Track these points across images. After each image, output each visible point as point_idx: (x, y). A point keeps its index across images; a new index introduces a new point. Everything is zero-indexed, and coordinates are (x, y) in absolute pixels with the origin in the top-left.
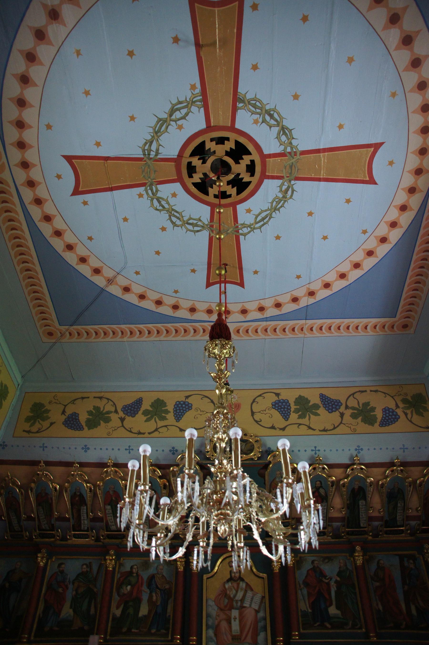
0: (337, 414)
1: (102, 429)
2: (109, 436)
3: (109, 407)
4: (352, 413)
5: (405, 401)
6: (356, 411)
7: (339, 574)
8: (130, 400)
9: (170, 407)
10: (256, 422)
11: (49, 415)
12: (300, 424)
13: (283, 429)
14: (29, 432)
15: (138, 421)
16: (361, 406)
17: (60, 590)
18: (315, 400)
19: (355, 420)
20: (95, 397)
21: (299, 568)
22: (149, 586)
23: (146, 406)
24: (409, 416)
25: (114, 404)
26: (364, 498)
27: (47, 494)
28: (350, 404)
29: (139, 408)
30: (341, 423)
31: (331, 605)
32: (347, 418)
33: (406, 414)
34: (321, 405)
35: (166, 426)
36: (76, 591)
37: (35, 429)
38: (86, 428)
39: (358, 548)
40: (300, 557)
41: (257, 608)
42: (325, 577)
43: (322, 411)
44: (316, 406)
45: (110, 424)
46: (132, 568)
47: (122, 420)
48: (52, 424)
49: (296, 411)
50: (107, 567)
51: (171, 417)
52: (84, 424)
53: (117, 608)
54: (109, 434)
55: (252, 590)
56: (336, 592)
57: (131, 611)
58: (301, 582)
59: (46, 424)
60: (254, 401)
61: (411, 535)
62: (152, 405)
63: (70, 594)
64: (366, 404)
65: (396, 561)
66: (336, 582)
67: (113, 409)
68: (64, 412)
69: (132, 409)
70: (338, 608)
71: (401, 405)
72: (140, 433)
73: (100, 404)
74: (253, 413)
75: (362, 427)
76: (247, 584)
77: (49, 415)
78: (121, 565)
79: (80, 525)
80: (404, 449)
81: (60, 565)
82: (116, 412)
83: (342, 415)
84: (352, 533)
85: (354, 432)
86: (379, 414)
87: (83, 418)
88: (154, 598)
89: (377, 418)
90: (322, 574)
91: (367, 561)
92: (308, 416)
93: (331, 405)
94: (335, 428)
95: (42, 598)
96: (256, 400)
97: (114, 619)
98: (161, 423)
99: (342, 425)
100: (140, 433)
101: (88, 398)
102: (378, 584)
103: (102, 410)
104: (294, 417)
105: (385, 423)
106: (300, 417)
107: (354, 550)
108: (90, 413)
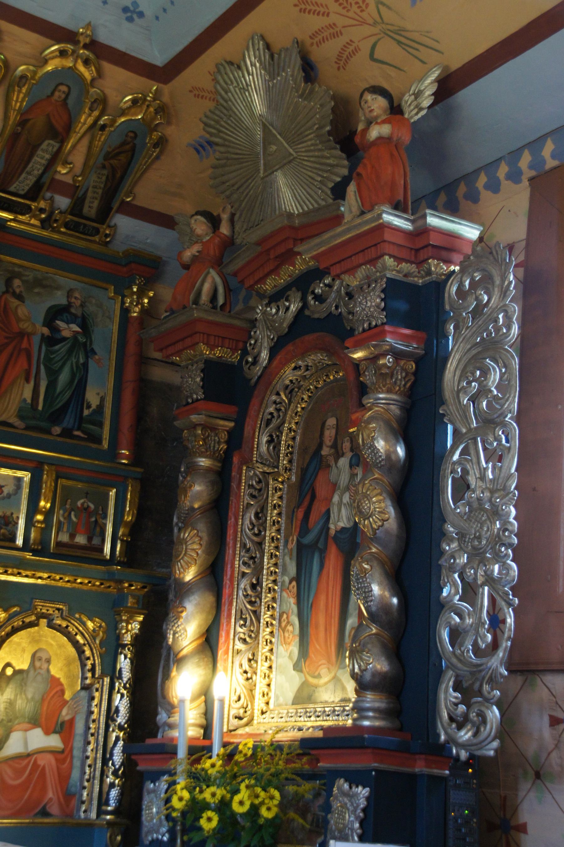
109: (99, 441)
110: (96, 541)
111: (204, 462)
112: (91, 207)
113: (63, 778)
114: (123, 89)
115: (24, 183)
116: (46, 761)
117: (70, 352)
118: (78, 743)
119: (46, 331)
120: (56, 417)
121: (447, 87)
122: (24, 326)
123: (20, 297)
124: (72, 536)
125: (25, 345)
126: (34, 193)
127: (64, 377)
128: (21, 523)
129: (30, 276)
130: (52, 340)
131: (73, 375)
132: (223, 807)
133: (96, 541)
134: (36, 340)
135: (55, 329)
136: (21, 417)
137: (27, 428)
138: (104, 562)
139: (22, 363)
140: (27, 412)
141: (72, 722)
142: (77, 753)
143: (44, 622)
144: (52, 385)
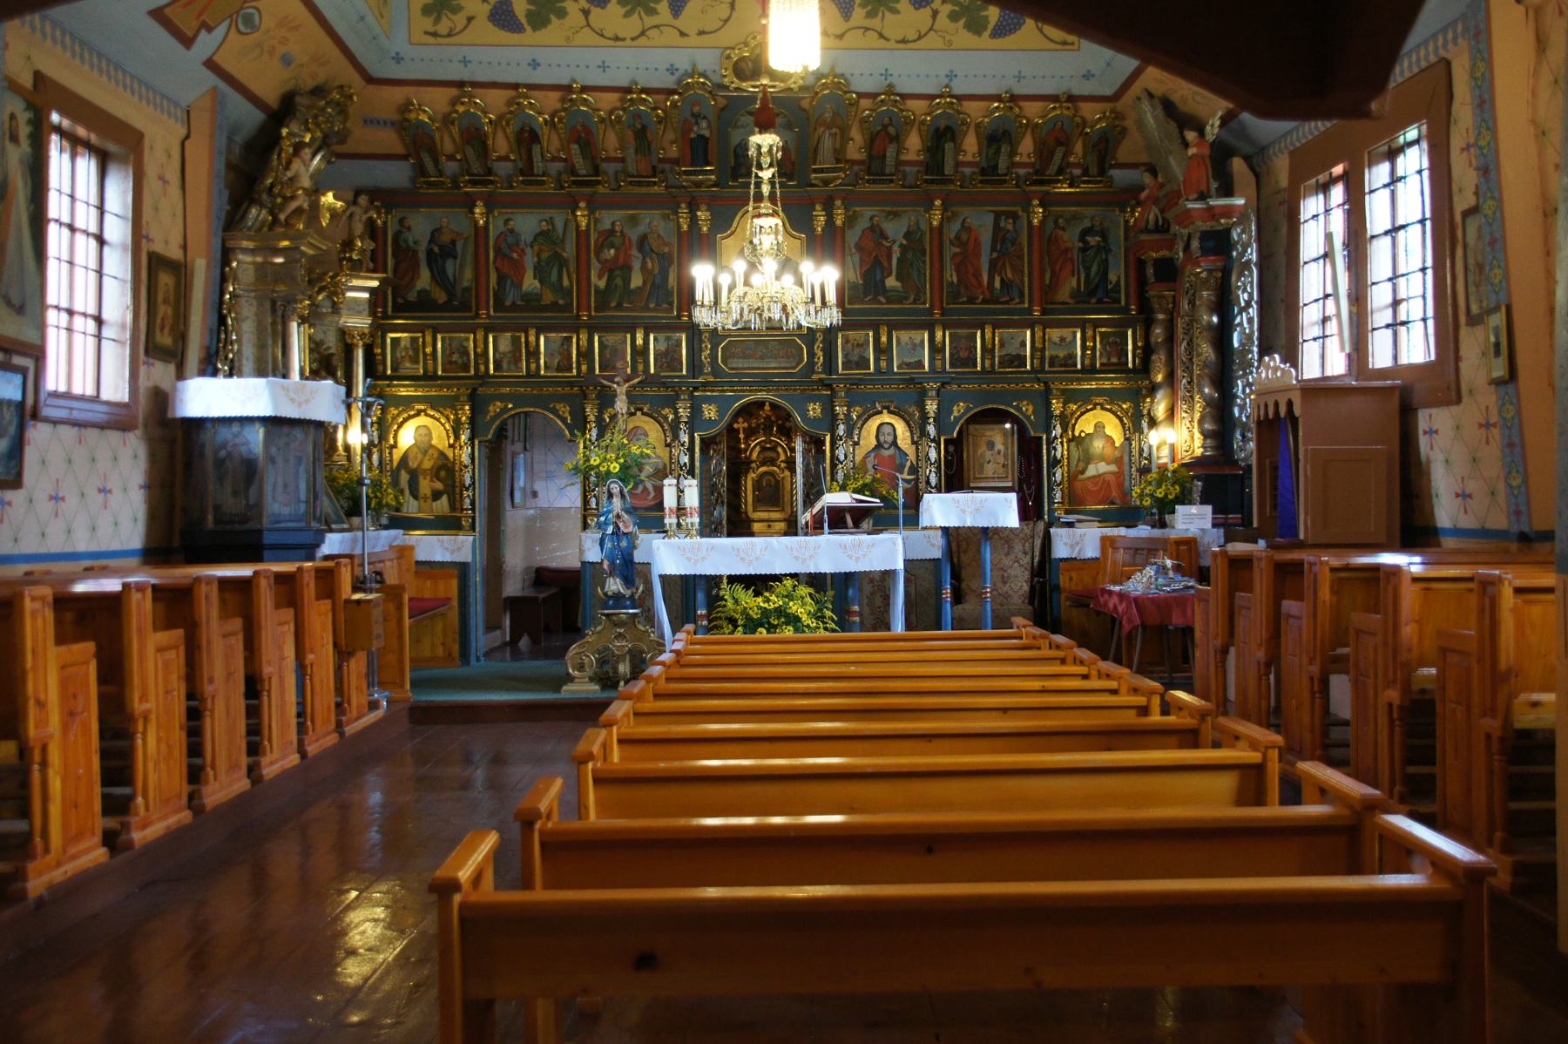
0: (927, 12)
1: (555, 30)
2: (568, 43)
4: (952, 12)
7: (907, 235)
12: (867, 29)
14: (435, 35)
17: (515, 255)
22: (641, 249)
26: (953, 139)
27: (478, 129)
31: (890, 274)
32: (943, 21)
35: (657, 27)
36: (538, 255)
39: (938, 203)
42: (886, 238)
45: (568, 21)
47: (586, 13)
48: (470, 19)
50: (578, 226)
52: (524, 21)
53: (600, 277)
54: (568, 39)
57: (619, 281)
59: (460, 20)
61: (1017, 186)
63: (529, 260)
66: (901, 245)
72: (617, 39)
75: (965, 38)
78: (597, 221)
79: (532, 169)
80: (1019, 77)
81: (506, 222)
83: (935, 14)
84: (932, 182)
85: (949, 47)
88: (650, 265)
90: (883, 236)
94: (920, 38)
95: (491, 266)
98: (649, 21)
100: (617, 39)
106: (871, 15)
107: (930, 207)
111: (1161, 316)
113: (1120, 486)
114: (1090, 111)
115: (1053, 169)
116: (1108, 478)
118: (1126, 468)
120: (1092, 293)
122: (1069, 245)
123: (1063, 229)
126: (1060, 171)
127: (1094, 270)
130: (1084, 250)
134: (1075, 251)
138: (1128, 371)
140: (1075, 294)
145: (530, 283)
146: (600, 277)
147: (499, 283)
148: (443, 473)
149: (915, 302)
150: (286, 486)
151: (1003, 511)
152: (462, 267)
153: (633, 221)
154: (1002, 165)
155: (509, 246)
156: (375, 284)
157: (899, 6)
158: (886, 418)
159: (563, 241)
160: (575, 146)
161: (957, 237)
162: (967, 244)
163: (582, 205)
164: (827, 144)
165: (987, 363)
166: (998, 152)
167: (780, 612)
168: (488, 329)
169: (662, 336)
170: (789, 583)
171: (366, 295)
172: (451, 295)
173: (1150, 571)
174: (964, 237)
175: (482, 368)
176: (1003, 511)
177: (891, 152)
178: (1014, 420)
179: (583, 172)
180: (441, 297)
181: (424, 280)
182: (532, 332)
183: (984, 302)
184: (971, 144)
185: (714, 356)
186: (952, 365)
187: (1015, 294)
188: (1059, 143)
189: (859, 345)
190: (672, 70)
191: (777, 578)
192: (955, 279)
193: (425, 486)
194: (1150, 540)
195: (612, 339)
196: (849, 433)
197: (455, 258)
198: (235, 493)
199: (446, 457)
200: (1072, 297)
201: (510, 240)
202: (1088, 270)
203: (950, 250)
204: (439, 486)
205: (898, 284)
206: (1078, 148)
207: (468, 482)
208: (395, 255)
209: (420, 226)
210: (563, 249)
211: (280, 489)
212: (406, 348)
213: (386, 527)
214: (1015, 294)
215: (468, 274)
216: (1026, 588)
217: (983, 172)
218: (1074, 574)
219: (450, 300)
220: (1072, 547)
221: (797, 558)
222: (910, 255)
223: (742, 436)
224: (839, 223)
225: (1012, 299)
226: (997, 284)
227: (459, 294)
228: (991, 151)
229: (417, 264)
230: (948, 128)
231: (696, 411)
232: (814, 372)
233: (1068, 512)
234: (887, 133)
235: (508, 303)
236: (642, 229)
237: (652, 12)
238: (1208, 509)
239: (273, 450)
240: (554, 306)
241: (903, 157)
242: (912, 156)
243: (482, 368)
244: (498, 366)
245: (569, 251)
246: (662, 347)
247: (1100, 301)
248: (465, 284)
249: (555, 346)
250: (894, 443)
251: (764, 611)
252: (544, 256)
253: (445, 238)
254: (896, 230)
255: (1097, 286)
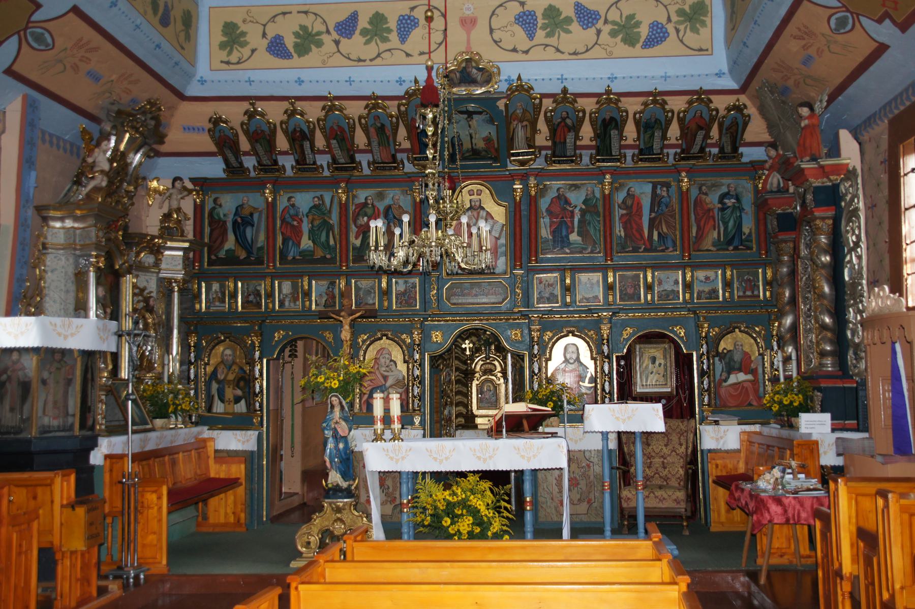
0: (592, 31)
2: (324, 64)
3: (319, 27)
4: (612, 30)
5: (681, 12)
6: (616, 27)
7: (584, 202)
8: (342, 16)
9: (393, 24)
10: (495, 42)
11: (248, 38)
12: (547, 46)
13: (526, 52)
14: (228, 63)
15: (355, 44)
16: (624, 19)
17: (295, 223)
18: (568, 11)
19: (613, 39)
20: (299, 12)
21: (542, 196)
23: (363, 22)
24: (681, 34)
25: (325, 21)
28: (610, 17)
29: (355, 26)
30: (596, 43)
31: (573, 232)
33: (678, 31)
34: (575, 19)
35: (389, 50)
36: (312, 223)
37: (234, 58)
38: (295, 55)
40: (545, 185)
41: (497, 236)
42: (570, 204)
43: (575, 27)
44: (568, 20)
45: (324, 49)
46: (366, 199)
47: (337, 43)
48: (253, 51)
49: (544, 28)
50: (341, 200)
51: (394, 37)
52: (292, 50)
53: (356, 238)
54: (324, 62)
55: (492, 218)
56: (579, 221)
58: (544, 210)
59: (246, 52)
60: (493, 13)
62: (371, 23)
63: (306, 227)
64: (631, 17)
65: (648, 188)
66: (581, 210)
67: (324, 29)
68: (264, 35)
69: (347, 27)
70: (578, 235)
71: (674, 18)
72: (360, 60)
73: (307, 21)
74: (491, 31)
76: (488, 213)
77: (248, 38)
78: (354, 197)
82: (328, 32)
83: (599, 32)
84: (603, 161)
85: (610, 56)
86: (644, 31)
87: (290, 42)
89: (640, 37)
90: (567, 202)
91: (615, 189)
92: (557, 34)
93: (587, 17)
94: (587, 51)
96: (497, 12)
97: (354, 248)
98: (384, 46)
99: (597, 46)
100: (360, 60)
101: (290, 13)
102: (624, 212)
103: (310, 30)
104: (540, 35)
105: (650, 43)
106: (548, 35)
108: (296, 34)
109: (750, 248)
110: (756, 293)
112: (728, 149)
115: (696, 149)
116: (745, 385)
117: (732, 213)
118: (760, 377)
119: (720, 206)
120: (729, 242)
121: (832, 98)
122: (710, 206)
123: (706, 194)
124: (744, 292)
125: (711, 214)
126: (702, 150)
127: (731, 224)
128: (721, 292)
129: (709, 183)
130: (722, 210)
131: (735, 222)
132: (780, 403)
133: (756, 293)
134: (716, 211)
135: (724, 204)
136: (714, 245)
137: (718, 250)
139: (711, 222)
141: (756, 369)
142: (761, 381)
143: (737, 330)
144: (726, 229)
145: (306, 243)
146: (356, 238)
147: (283, 244)
148: (242, 384)
149: (592, 252)
150: (55, 403)
151: (649, 418)
152: (258, 231)
153: (381, 196)
154: (656, 146)
155: (292, 217)
156: (186, 245)
157: (570, 28)
158: (571, 339)
159: (330, 212)
160: (334, 142)
161: (624, 202)
162: (632, 207)
163: (343, 185)
164: (520, 134)
165: (649, 297)
166: (652, 135)
167: (464, 504)
168: (274, 277)
169: (401, 281)
170: (471, 478)
171: (181, 253)
172: (249, 253)
173: (777, 472)
174: (629, 202)
175: (271, 305)
176: (649, 418)
177: (570, 138)
178: (673, 341)
179: (342, 161)
180: (243, 255)
181: (230, 243)
182: (306, 279)
183: (646, 250)
184: (630, 131)
185: (439, 296)
186: (621, 299)
187: (669, 243)
188: (702, 129)
189: (550, 285)
190: (400, 82)
191: (463, 475)
192: (623, 234)
193: (229, 393)
194: (779, 438)
195: (365, 283)
196: (542, 351)
197: (253, 226)
198: (12, 410)
199: (245, 372)
200: (714, 245)
201: (292, 212)
202: (726, 224)
203: (618, 213)
204: (239, 392)
205: (579, 239)
206: (715, 132)
207: (257, 390)
208: (210, 224)
209: (229, 203)
210: (330, 218)
211: (50, 405)
212: (216, 292)
213: (196, 424)
214: (669, 243)
215: (262, 237)
216: (682, 472)
217: (641, 152)
218: (719, 462)
219: (248, 257)
220: (717, 440)
221: (479, 458)
222: (588, 217)
223: (468, 353)
224: (533, 193)
225: (667, 248)
226: (655, 237)
227: (255, 251)
228: (647, 136)
229: (226, 230)
230: (612, 119)
231: (426, 336)
232: (515, 306)
233: (713, 412)
234: (566, 125)
235: (290, 258)
236: (388, 201)
237: (385, 40)
238: (827, 417)
239: (46, 375)
240: (323, 260)
241: (578, 143)
242: (586, 141)
243: (271, 305)
244: (282, 303)
245: (334, 219)
246: (402, 288)
247: (736, 248)
248: (259, 245)
249: (324, 289)
250: (578, 359)
251: (449, 503)
252: (317, 223)
253: (246, 212)
254: (577, 198)
255: (733, 237)
